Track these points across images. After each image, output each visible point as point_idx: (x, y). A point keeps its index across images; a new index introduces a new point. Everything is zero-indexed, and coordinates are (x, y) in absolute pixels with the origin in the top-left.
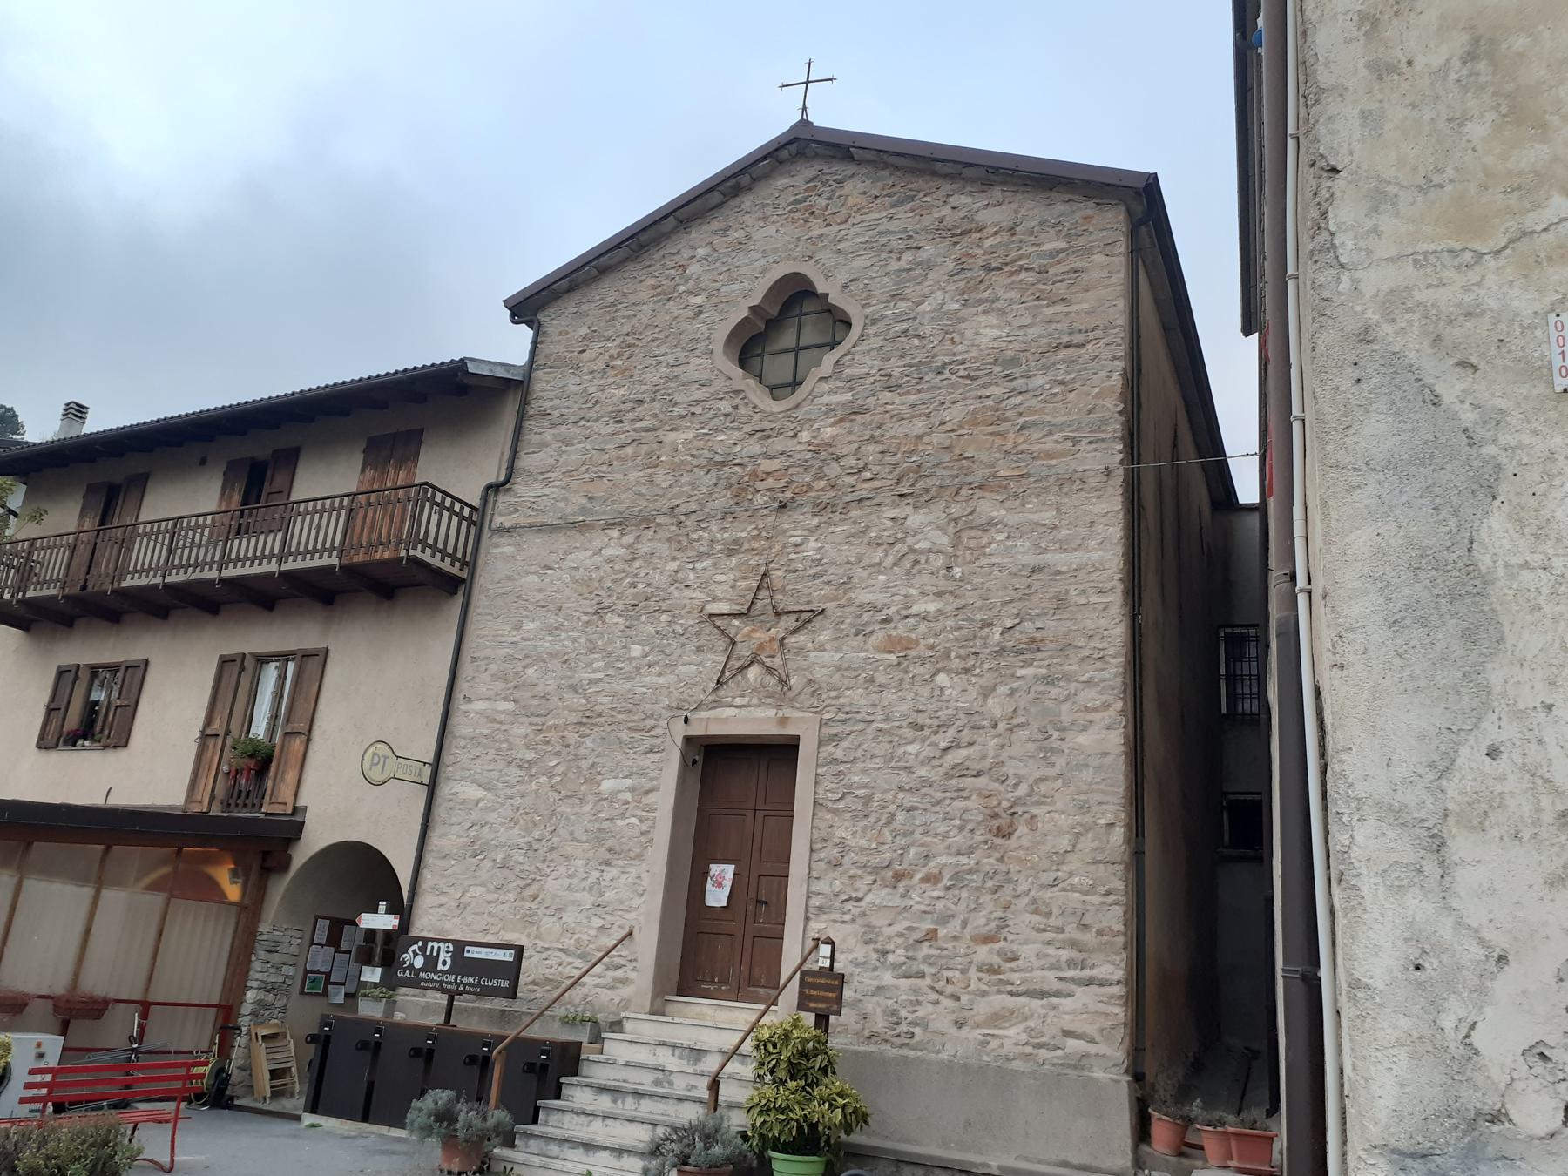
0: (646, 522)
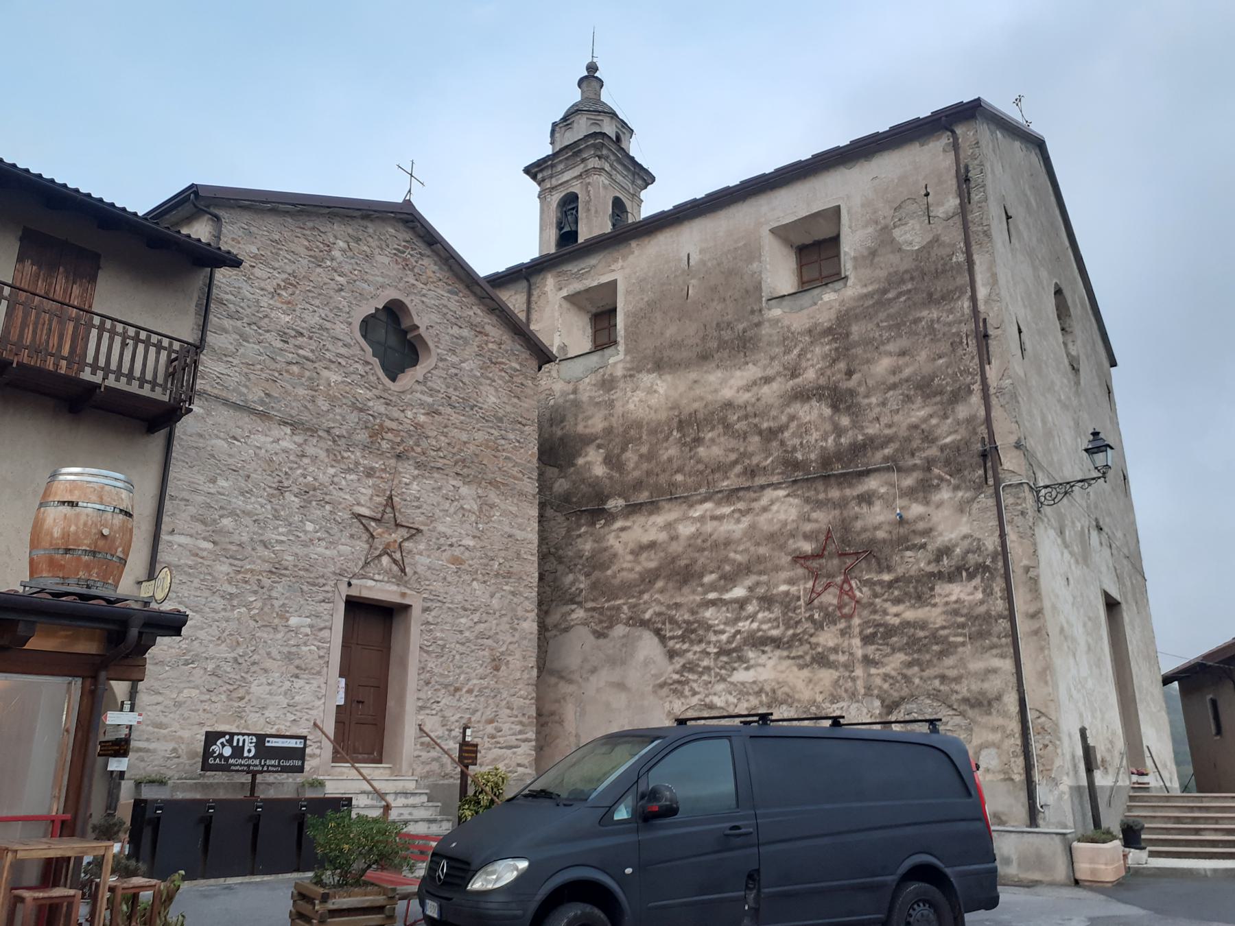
0: (312, 431)
